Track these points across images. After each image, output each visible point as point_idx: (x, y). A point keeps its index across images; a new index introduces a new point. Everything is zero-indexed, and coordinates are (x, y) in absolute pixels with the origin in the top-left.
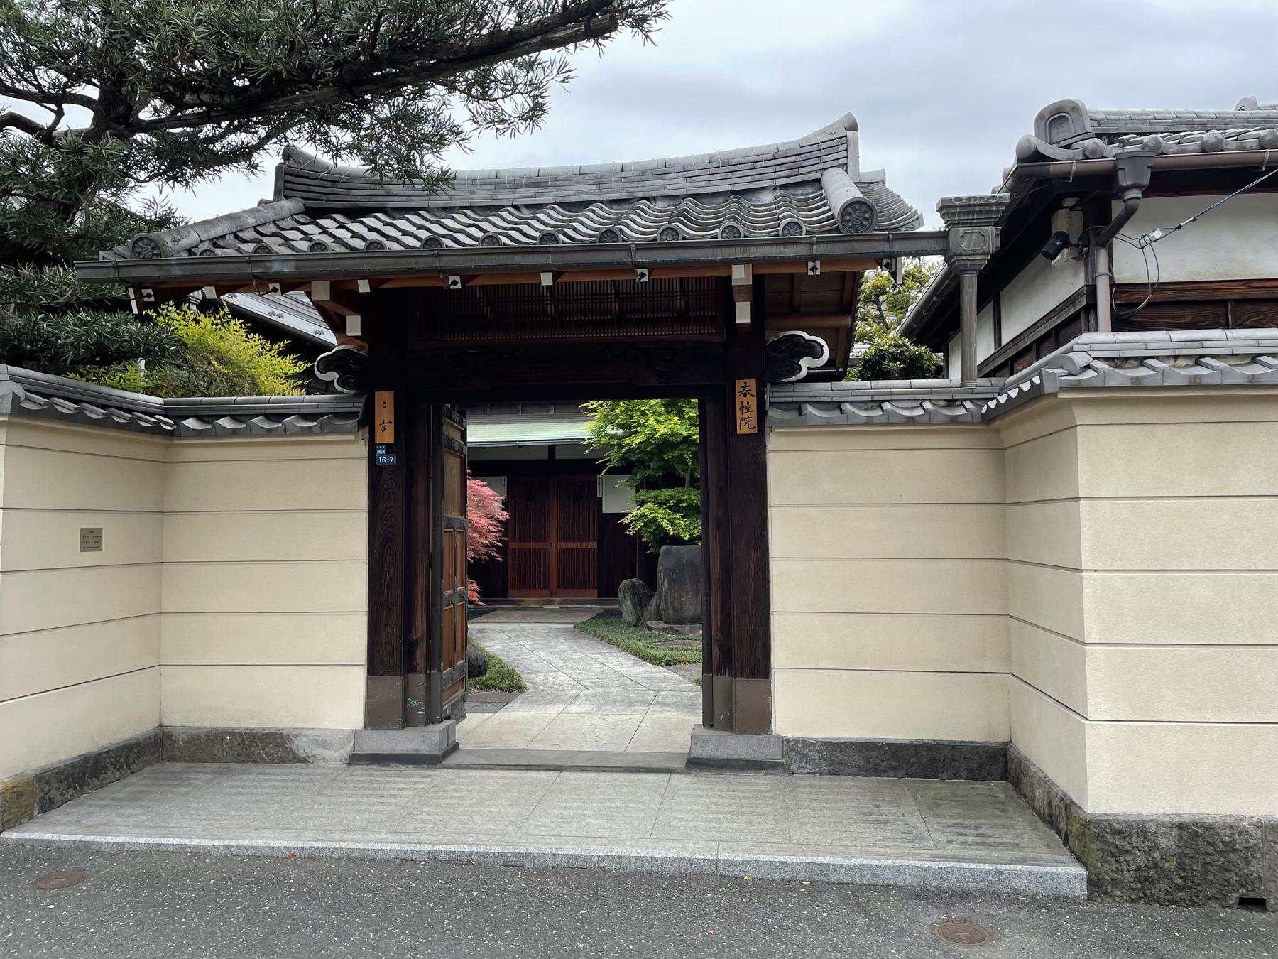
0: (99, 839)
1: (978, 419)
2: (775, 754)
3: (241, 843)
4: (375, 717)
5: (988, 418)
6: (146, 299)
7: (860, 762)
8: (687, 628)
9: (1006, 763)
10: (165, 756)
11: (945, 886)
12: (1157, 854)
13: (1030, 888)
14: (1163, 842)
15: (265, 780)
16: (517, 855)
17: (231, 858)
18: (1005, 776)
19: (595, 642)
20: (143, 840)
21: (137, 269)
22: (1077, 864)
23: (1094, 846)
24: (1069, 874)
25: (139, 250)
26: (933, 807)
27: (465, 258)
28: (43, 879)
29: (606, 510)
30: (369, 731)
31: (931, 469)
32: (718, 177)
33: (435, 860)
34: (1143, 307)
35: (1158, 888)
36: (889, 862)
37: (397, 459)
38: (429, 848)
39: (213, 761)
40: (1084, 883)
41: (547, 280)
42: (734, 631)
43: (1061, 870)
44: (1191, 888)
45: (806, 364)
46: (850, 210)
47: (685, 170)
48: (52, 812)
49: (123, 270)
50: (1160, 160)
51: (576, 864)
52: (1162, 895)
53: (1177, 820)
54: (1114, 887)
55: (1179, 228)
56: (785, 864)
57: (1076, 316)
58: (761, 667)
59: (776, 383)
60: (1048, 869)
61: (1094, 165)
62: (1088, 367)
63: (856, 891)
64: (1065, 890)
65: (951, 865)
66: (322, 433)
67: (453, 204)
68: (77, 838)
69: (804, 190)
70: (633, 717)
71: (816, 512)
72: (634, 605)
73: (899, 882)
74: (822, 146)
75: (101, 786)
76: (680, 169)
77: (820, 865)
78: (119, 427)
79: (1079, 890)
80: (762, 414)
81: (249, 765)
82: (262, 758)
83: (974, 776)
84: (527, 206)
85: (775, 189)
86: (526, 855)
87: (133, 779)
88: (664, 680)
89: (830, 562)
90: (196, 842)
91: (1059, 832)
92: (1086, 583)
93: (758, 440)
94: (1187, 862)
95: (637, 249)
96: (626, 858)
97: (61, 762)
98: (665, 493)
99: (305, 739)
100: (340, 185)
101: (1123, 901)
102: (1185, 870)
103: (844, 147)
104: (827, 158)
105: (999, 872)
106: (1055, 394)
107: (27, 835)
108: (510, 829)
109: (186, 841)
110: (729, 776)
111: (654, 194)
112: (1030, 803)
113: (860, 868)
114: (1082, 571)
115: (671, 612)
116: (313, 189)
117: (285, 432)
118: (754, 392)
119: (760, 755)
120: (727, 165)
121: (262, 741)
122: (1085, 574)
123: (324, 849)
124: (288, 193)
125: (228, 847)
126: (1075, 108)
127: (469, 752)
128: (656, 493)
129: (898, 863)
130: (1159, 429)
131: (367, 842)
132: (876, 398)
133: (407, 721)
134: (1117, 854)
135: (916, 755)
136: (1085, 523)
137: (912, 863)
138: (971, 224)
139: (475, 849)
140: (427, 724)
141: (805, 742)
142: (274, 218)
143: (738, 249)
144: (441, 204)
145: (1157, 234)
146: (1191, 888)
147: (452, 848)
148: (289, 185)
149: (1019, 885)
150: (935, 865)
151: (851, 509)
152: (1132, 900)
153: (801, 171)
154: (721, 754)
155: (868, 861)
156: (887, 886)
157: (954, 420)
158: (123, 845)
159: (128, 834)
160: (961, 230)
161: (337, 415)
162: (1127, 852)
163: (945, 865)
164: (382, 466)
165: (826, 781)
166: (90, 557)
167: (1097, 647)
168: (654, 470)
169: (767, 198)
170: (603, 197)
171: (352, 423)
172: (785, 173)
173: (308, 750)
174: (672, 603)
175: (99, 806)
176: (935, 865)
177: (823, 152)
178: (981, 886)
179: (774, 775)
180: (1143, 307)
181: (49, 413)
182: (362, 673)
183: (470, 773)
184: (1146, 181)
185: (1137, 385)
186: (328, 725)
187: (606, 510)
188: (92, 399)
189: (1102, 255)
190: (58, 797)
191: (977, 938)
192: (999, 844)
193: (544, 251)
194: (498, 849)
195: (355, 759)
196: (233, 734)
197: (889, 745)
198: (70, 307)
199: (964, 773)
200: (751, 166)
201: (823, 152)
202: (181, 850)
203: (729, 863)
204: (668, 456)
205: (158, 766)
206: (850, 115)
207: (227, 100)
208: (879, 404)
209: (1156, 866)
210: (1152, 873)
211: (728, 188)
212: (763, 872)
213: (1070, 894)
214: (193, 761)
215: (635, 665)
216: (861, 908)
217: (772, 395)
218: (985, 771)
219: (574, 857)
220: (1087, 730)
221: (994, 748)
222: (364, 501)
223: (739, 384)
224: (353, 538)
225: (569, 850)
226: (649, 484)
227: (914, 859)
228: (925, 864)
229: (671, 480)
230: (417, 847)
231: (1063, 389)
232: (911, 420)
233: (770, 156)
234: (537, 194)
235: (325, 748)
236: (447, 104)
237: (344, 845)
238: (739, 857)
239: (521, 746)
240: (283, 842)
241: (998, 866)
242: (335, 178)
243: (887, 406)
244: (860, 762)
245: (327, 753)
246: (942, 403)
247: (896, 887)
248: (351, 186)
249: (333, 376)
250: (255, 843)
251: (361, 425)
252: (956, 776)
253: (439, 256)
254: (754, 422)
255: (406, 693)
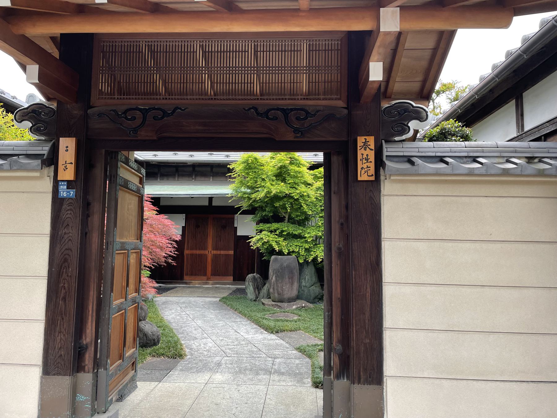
8: (286, 304)
19: (231, 313)
29: (239, 234)
42: (353, 344)
45: (413, 124)
58: (375, 376)
66: (11, 169)
71: (421, 245)
72: (254, 289)
80: (379, 163)
88: (277, 347)
89: (433, 288)
93: (376, 183)
98: (275, 226)
115: (276, 295)
118: (372, 147)
128: (268, 225)
132: (471, 154)
151: (450, 244)
157: (541, 173)
164: (63, 199)
168: (268, 212)
174: (277, 290)
182: (36, 373)
187: (239, 234)
204: (277, 204)
208: (474, 160)
215: (256, 332)
217: (388, 150)
222: (47, 228)
223: (361, 140)
226: (264, 220)
229: (278, 219)
232: (506, 172)
254: (372, 171)
255: (74, 390)
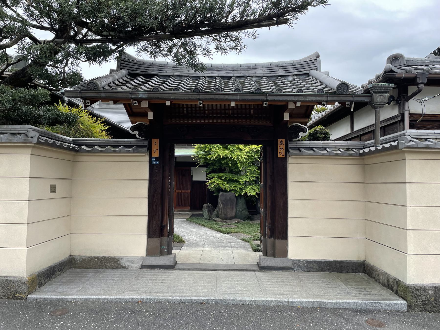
0: (66, 297)
1: (358, 155)
2: (289, 265)
3: (121, 297)
4: (150, 252)
5: (361, 155)
6: (87, 104)
7: (317, 267)
8: (229, 221)
9: (364, 267)
10: (72, 266)
11: (363, 308)
12: (428, 296)
13: (390, 308)
14: (430, 293)
15: (114, 275)
16: (220, 300)
17: (117, 302)
18: (364, 271)
19: (197, 226)
20: (84, 297)
21: (88, 94)
22: (402, 300)
23: (410, 294)
24: (402, 304)
25: (89, 86)
26: (347, 282)
27: (212, 96)
28: (52, 312)
29: (194, 179)
30: (148, 257)
31: (342, 171)
32: (274, 70)
33: (191, 302)
34: (418, 122)
35: (428, 307)
36: (345, 301)
37: (159, 162)
38: (189, 298)
39: (91, 268)
40: (406, 306)
41: (233, 104)
42: (276, 224)
43: (399, 302)
44: (438, 307)
45: (301, 134)
46: (340, 86)
47: (263, 67)
48: (42, 288)
49: (83, 94)
50: (430, 75)
51: (240, 303)
52: (430, 309)
53: (434, 286)
54: (415, 307)
55: (434, 97)
56: (311, 302)
57: (396, 123)
58: (284, 236)
59: (290, 141)
60: (395, 302)
61: (409, 75)
62: (411, 141)
63: (336, 311)
64: (400, 309)
65: (365, 301)
66: (134, 152)
67: (182, 74)
68: (58, 297)
69: (303, 77)
70: (229, 252)
71: (303, 184)
72: (208, 212)
73: (348, 307)
74: (309, 62)
75: (55, 278)
76: (261, 67)
77: (323, 302)
78: (64, 148)
79: (405, 308)
80: (287, 151)
81: (104, 269)
82: (109, 267)
83: (354, 272)
84: (208, 77)
85: (293, 76)
86: (223, 300)
87: (65, 275)
88: (230, 239)
89: (308, 201)
90: (104, 297)
91: (393, 291)
92: (408, 210)
94: (437, 298)
95: (269, 95)
96: (258, 301)
97: (44, 269)
98: (221, 175)
99: (125, 260)
100: (141, 65)
101: (418, 311)
102: (436, 301)
103: (316, 63)
104: (310, 66)
105: (380, 303)
106: (401, 149)
107: (38, 296)
108: (213, 291)
109: (100, 297)
110: (274, 272)
111: (253, 75)
112: (378, 281)
113: (336, 303)
114: (406, 206)
115: (223, 215)
116: (131, 66)
117: (120, 152)
118: (284, 144)
119: (284, 265)
120: (277, 67)
121: (109, 260)
122: (407, 207)
123: (151, 299)
124: (122, 67)
125: (116, 299)
126: (401, 56)
127: (181, 264)
128: (217, 174)
129: (348, 301)
130: (431, 161)
131: (167, 296)
132: (324, 147)
133: (161, 253)
134: (416, 296)
135: (335, 265)
136: (408, 191)
137: (352, 301)
138: (381, 93)
139: (205, 298)
140: (160, 256)
141: (299, 261)
142: (121, 76)
143: (303, 97)
144: (178, 74)
145: (427, 99)
146: (438, 307)
147: (197, 298)
148: (122, 65)
149: (386, 307)
150: (360, 301)
151: (315, 183)
152: (421, 311)
153: (302, 70)
154: (271, 265)
155: (338, 301)
156: (345, 309)
157: (351, 155)
158: (76, 299)
159: (77, 295)
160: (378, 95)
161: (138, 146)
162: (419, 296)
163: (363, 301)
164: (154, 165)
165: (307, 274)
166: (53, 195)
167: (411, 231)
168: (216, 166)
169: (290, 78)
170: (235, 75)
171: (144, 149)
172: (297, 71)
173: (126, 264)
174: (224, 212)
175: (59, 285)
176: (360, 301)
177: (309, 64)
178: (374, 308)
179: (289, 272)
180: (418, 122)
181: (46, 144)
182: (145, 237)
183: (186, 272)
184: (426, 82)
185: (427, 147)
186: (132, 255)
187: (194, 179)
188: (55, 138)
189: (407, 103)
190: (43, 282)
191: (381, 325)
192: (376, 294)
193: (237, 95)
194: (213, 298)
195: (143, 267)
196: (98, 258)
197: (327, 262)
198: (42, 104)
199: (351, 271)
200: (285, 67)
201: (309, 64)
202: (98, 300)
203: (293, 302)
204: (223, 162)
205: (70, 270)
206: (317, 53)
207: (121, 35)
208: (325, 149)
209: (428, 300)
210: (427, 302)
211: (278, 75)
212: (304, 305)
213: (402, 310)
214: (83, 268)
215: (216, 234)
216: (341, 316)
217: (291, 145)
218: (359, 270)
219: (240, 301)
220: (408, 257)
221: (360, 263)
222: (147, 176)
223: (279, 141)
224: (143, 189)
225: (238, 298)
226: (214, 171)
227: (353, 300)
228: (357, 301)
229: (221, 170)
230: (185, 298)
231: (405, 148)
232: (337, 155)
233: (291, 65)
234: (211, 73)
235: (132, 263)
236: (200, 42)
237: (158, 298)
238: (296, 300)
239: (198, 262)
240: (136, 297)
241: (380, 302)
242: (139, 63)
243: (328, 150)
244: (317, 267)
245: (133, 265)
246: (345, 149)
247: (347, 309)
248: (145, 66)
249: (136, 133)
250: (126, 297)
251: (148, 150)
252: (348, 272)
253: (199, 94)
254: (284, 153)
255: (161, 244)
